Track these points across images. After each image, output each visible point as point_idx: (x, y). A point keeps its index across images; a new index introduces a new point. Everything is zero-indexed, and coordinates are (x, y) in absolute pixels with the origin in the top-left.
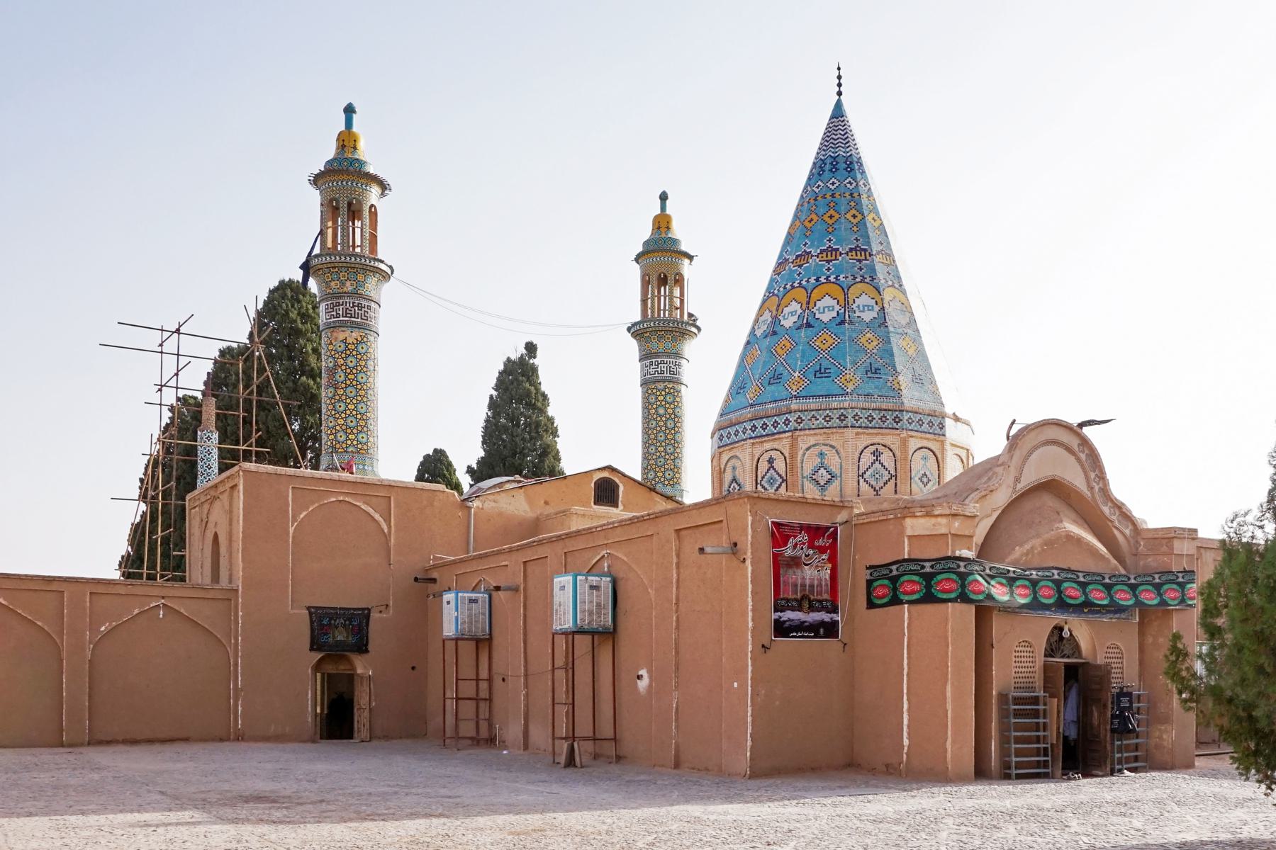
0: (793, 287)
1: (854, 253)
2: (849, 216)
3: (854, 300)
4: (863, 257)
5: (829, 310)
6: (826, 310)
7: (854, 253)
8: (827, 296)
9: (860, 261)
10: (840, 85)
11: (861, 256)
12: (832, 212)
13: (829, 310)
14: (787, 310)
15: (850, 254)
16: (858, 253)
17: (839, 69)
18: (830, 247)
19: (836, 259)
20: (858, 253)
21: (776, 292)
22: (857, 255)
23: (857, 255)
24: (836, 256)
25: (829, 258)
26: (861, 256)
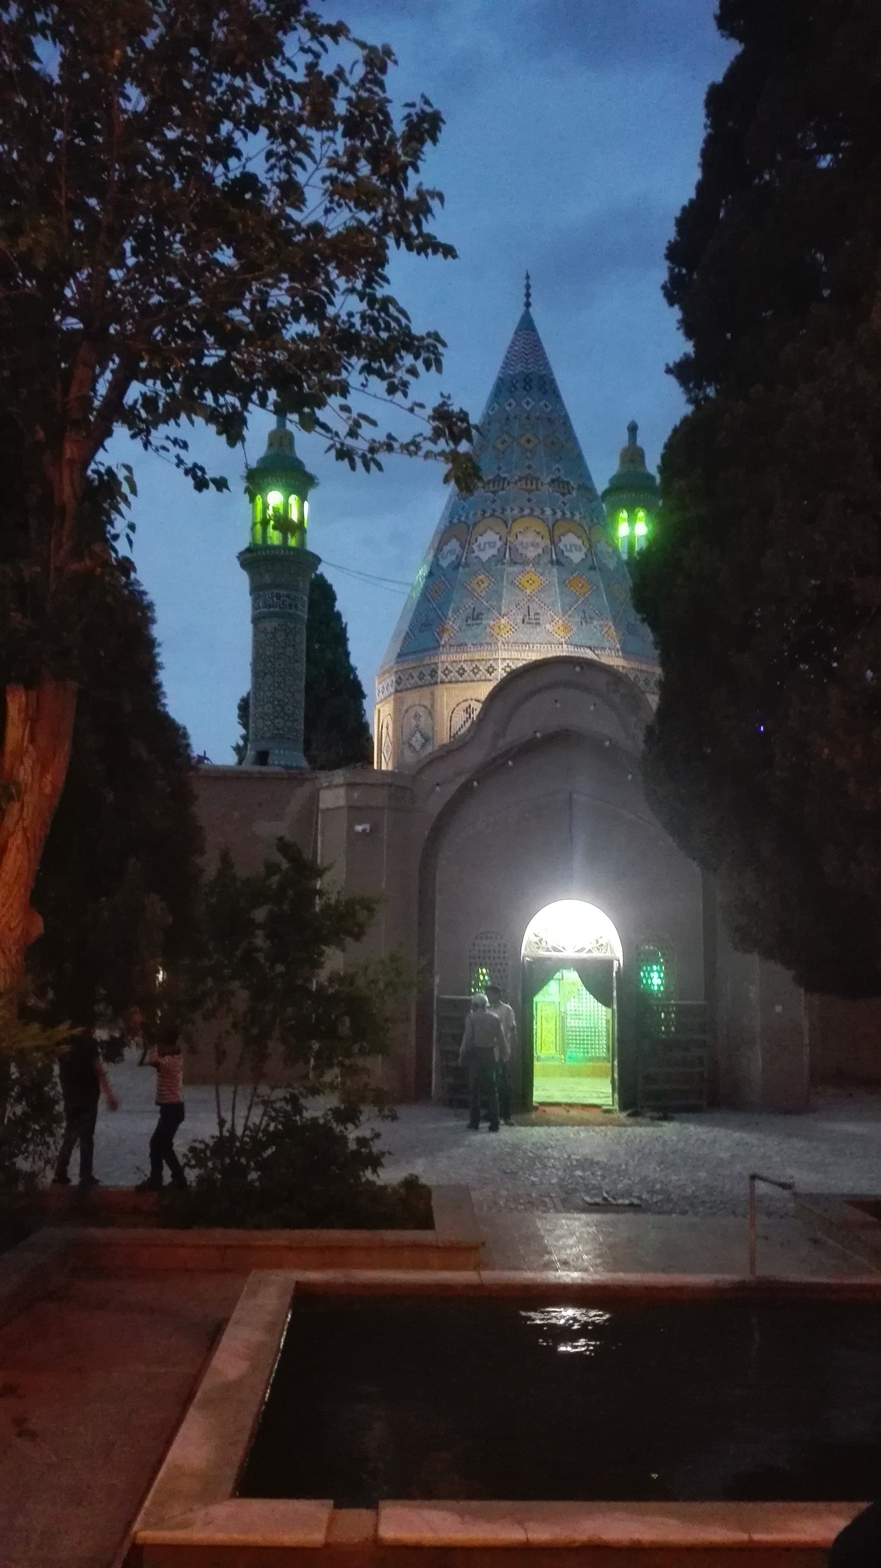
0: (459, 520)
1: (523, 482)
2: (523, 441)
3: (517, 535)
4: (534, 487)
5: (490, 547)
6: (487, 546)
7: (523, 482)
8: (489, 530)
9: (530, 491)
10: (528, 295)
11: (532, 484)
12: (505, 437)
13: (490, 547)
14: (447, 548)
15: (519, 484)
16: (529, 482)
17: (528, 277)
18: (498, 475)
19: (503, 489)
20: (529, 482)
21: (463, 519)
22: (526, 484)
23: (526, 484)
24: (503, 486)
25: (496, 488)
26: (532, 484)
